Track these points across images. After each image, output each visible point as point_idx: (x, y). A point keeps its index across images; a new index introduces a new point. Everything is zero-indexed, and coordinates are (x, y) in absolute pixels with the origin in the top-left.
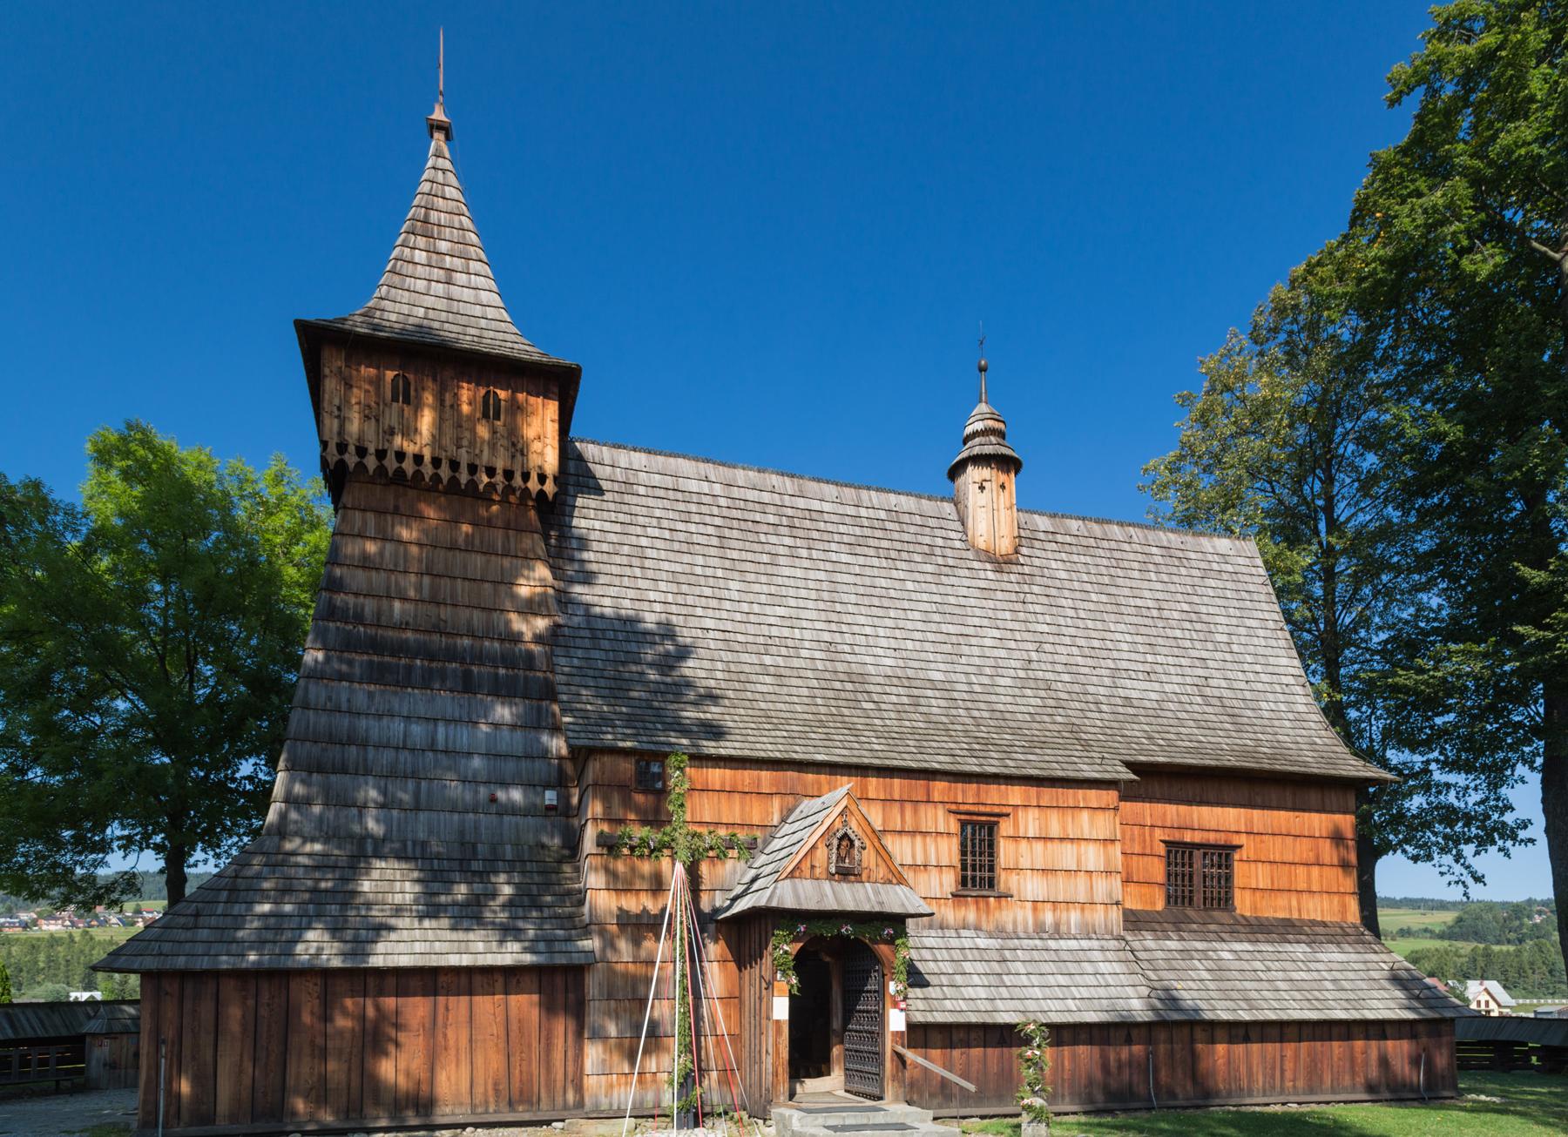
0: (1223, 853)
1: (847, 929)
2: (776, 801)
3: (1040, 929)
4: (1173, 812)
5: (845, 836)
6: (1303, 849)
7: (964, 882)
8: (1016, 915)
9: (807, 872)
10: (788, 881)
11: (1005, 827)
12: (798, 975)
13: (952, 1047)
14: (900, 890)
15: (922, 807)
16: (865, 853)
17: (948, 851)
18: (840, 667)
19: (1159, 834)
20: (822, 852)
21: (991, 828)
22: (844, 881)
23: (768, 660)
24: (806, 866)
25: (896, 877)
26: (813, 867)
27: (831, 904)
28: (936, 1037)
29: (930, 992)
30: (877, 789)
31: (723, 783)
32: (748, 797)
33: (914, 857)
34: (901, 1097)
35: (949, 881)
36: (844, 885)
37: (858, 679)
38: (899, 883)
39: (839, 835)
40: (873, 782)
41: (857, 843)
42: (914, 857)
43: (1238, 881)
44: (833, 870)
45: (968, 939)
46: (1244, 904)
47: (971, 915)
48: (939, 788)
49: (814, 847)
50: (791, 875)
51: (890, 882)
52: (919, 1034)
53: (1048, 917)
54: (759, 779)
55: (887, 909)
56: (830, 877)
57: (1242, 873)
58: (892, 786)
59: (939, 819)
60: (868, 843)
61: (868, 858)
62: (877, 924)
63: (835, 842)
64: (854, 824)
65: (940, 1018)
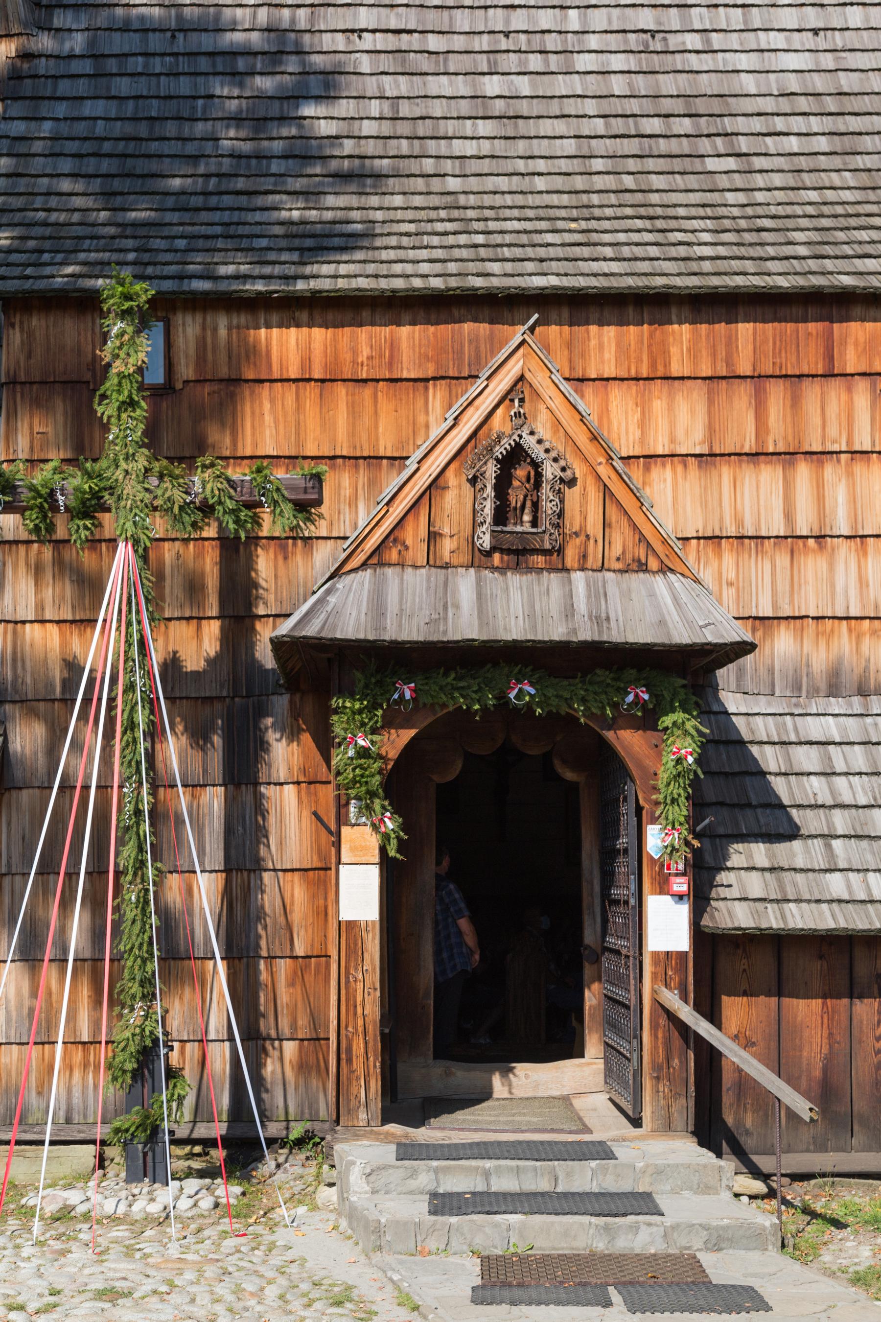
1: (522, 692)
2: (436, 395)
5: (516, 455)
9: (418, 552)
10: (366, 575)
12: (396, 811)
13: (853, 992)
15: (811, 392)
16: (572, 495)
18: (668, 84)
20: (456, 500)
22: (517, 567)
23: (492, 86)
24: (415, 535)
25: (652, 556)
26: (433, 537)
27: (464, 626)
28: (810, 967)
29: (795, 852)
30: (694, 354)
31: (306, 362)
32: (367, 391)
33: (789, 516)
34: (691, 1128)
36: (515, 580)
37: (709, 112)
38: (665, 569)
39: (499, 451)
40: (682, 340)
41: (550, 470)
42: (789, 516)
44: (486, 541)
49: (436, 485)
50: (377, 559)
51: (642, 567)
52: (720, 962)
54: (393, 346)
55: (616, 634)
56: (480, 558)
58: (731, 342)
60: (579, 470)
61: (584, 508)
62: (602, 674)
63: (491, 470)
64: (543, 428)
65: (799, 918)
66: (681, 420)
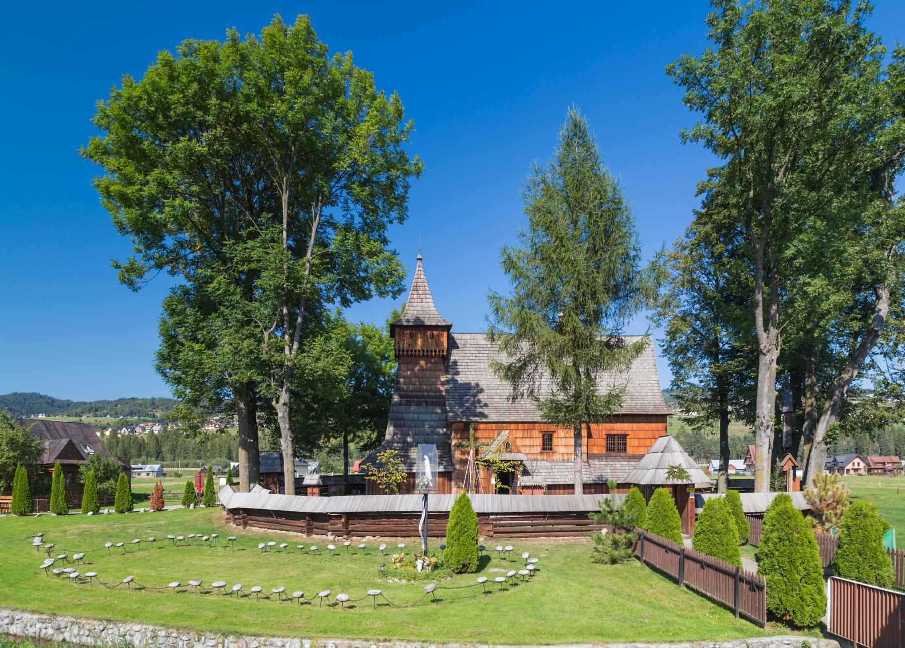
0: (624, 437)
3: (563, 460)
4: (608, 426)
6: (650, 434)
7: (543, 449)
8: (557, 457)
11: (555, 435)
14: (520, 454)
17: (539, 441)
19: (604, 432)
21: (551, 435)
35: (539, 449)
43: (628, 444)
45: (544, 463)
46: (630, 450)
47: (545, 457)
48: (537, 425)
53: (566, 457)
57: (629, 441)
59: (537, 433)
61: (513, 447)
66: (520, 434)
